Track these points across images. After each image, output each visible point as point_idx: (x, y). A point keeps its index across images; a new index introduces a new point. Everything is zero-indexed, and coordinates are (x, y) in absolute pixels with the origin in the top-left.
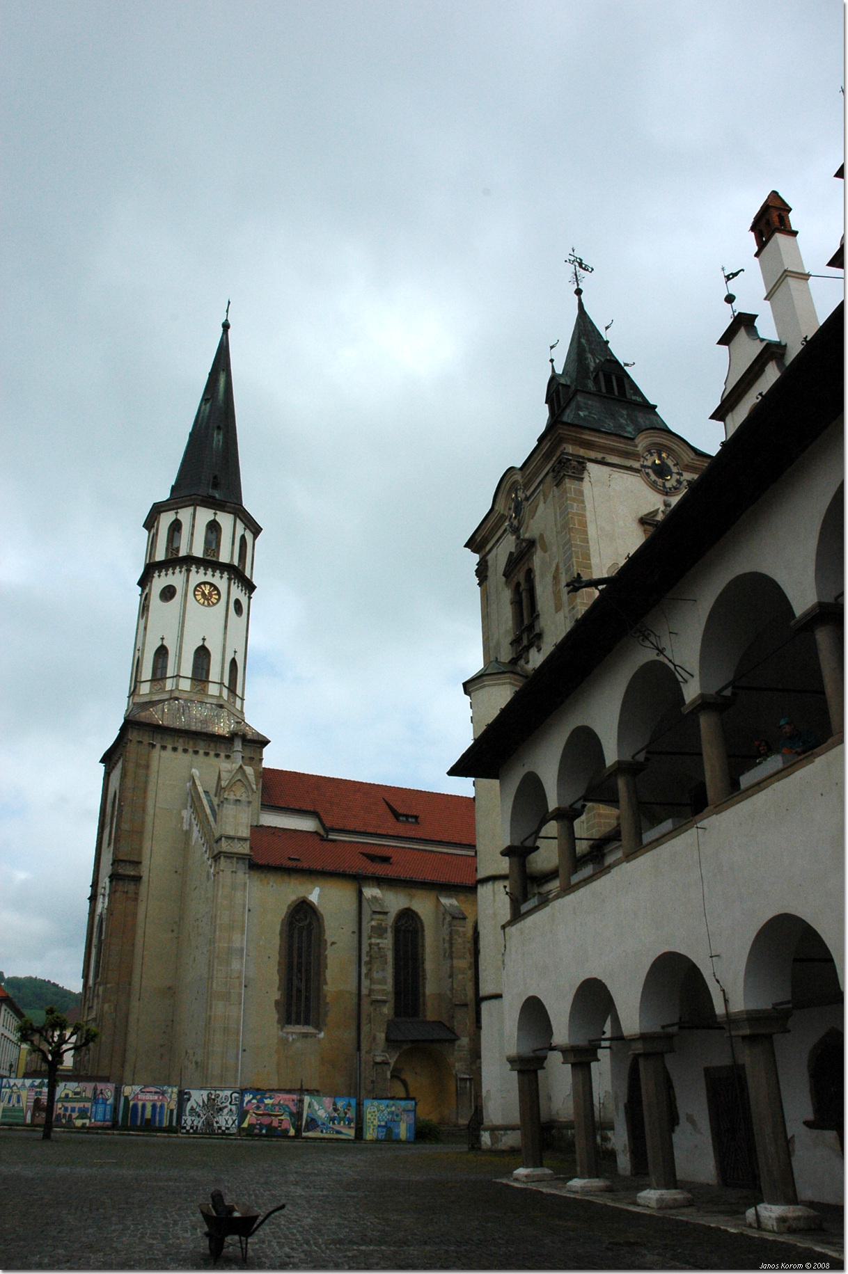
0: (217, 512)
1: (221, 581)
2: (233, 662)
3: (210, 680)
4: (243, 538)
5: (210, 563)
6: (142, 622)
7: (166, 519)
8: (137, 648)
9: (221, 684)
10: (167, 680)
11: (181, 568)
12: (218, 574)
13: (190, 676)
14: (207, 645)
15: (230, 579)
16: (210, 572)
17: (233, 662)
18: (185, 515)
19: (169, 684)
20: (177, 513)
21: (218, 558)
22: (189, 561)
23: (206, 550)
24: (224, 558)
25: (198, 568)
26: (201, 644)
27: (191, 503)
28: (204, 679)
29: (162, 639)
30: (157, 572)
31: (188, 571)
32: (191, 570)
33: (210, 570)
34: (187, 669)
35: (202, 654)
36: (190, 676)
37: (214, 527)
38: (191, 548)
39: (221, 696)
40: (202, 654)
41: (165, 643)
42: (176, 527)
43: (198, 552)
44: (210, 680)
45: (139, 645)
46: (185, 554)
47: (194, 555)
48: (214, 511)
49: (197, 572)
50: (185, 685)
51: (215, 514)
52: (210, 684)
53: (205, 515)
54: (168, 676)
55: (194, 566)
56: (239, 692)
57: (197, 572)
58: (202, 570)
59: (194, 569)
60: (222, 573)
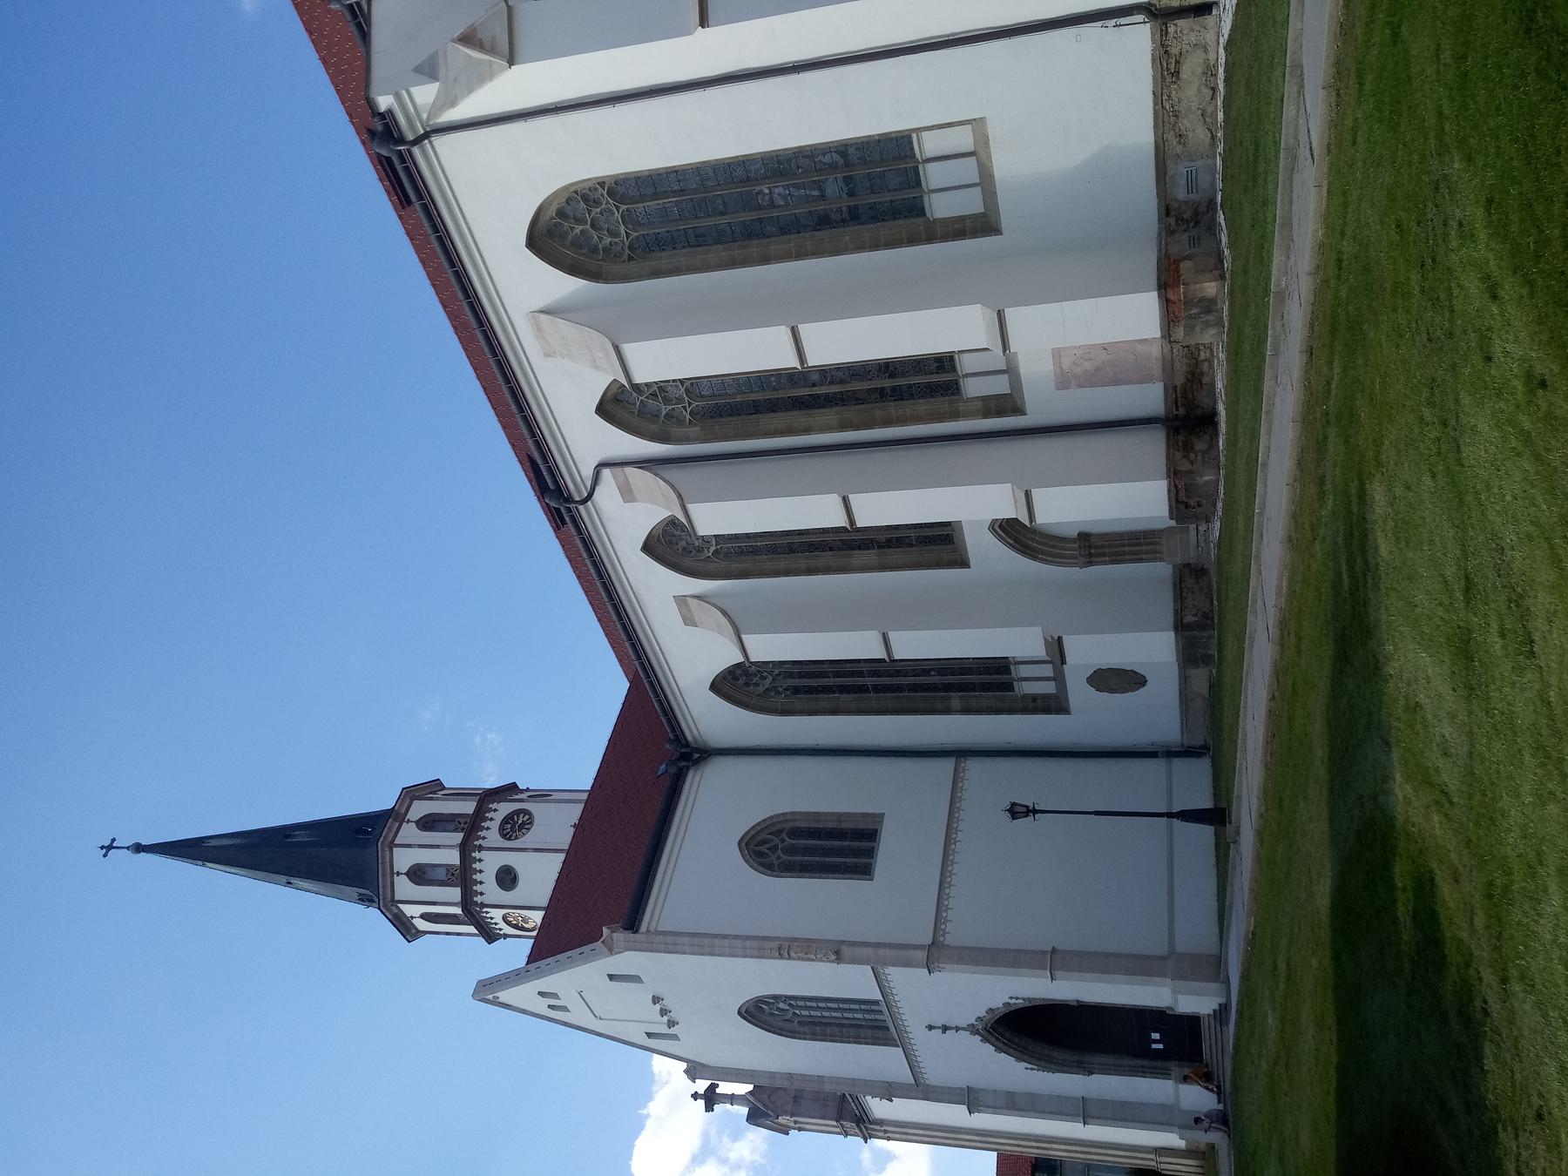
0: (395, 871)
1: (489, 864)
5: (463, 877)
12: (477, 866)
15: (480, 848)
20: (412, 918)
24: (453, 857)
31: (483, 905)
37: (419, 875)
43: (455, 893)
46: (460, 909)
47: (460, 900)
51: (398, 874)
57: (482, 894)
59: (478, 899)
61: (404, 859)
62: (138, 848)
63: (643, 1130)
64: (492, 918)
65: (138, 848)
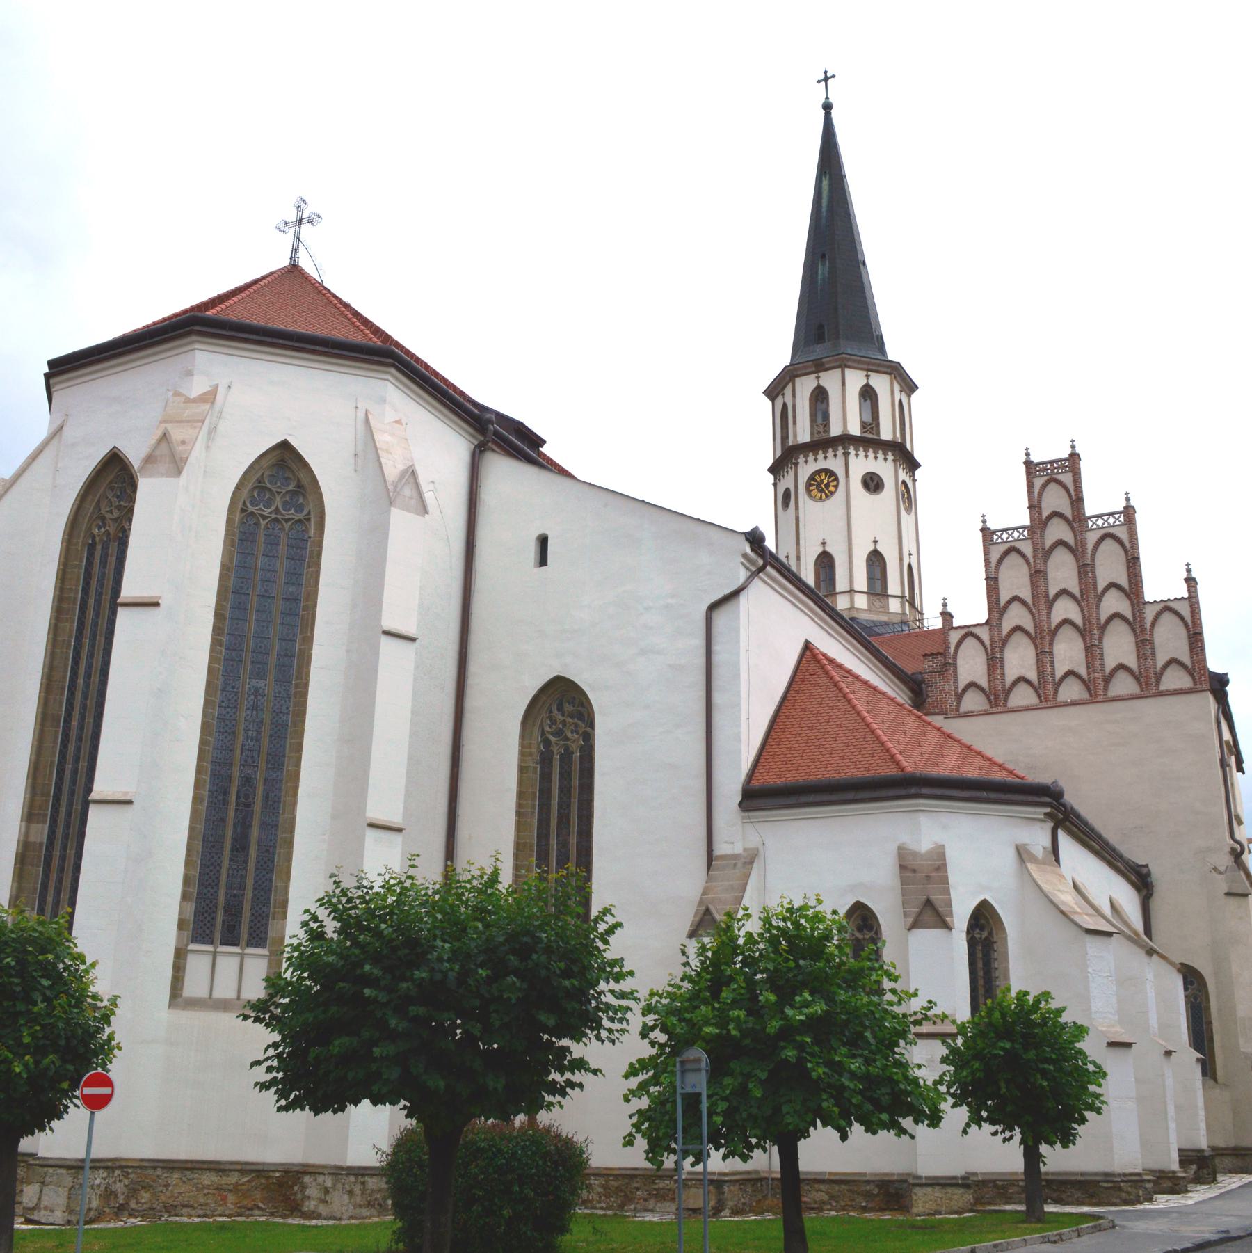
0: (869, 373)
1: (884, 467)
2: (910, 566)
3: (889, 593)
4: (900, 402)
5: (869, 441)
7: (805, 386)
9: (903, 597)
11: (835, 450)
13: (866, 590)
14: (880, 548)
16: (871, 454)
17: (910, 566)
18: (830, 380)
20: (818, 378)
21: (878, 433)
22: (846, 440)
23: (864, 425)
24: (886, 434)
25: (857, 450)
27: (838, 363)
28: (879, 591)
29: (824, 544)
30: (801, 456)
31: (846, 454)
32: (849, 453)
33: (871, 450)
34: (861, 583)
35: (876, 560)
36: (866, 590)
37: (868, 394)
39: (904, 613)
40: (876, 560)
41: (828, 549)
42: (820, 396)
43: (855, 429)
44: (889, 593)
48: (865, 373)
49: (857, 455)
50: (861, 602)
51: (868, 376)
52: (890, 599)
53: (856, 380)
54: (838, 590)
55: (852, 447)
56: (917, 604)
57: (857, 455)
58: (861, 453)
59: (852, 451)
60: (885, 454)
61: (881, 383)
63: (1227, 696)
64: (825, 458)
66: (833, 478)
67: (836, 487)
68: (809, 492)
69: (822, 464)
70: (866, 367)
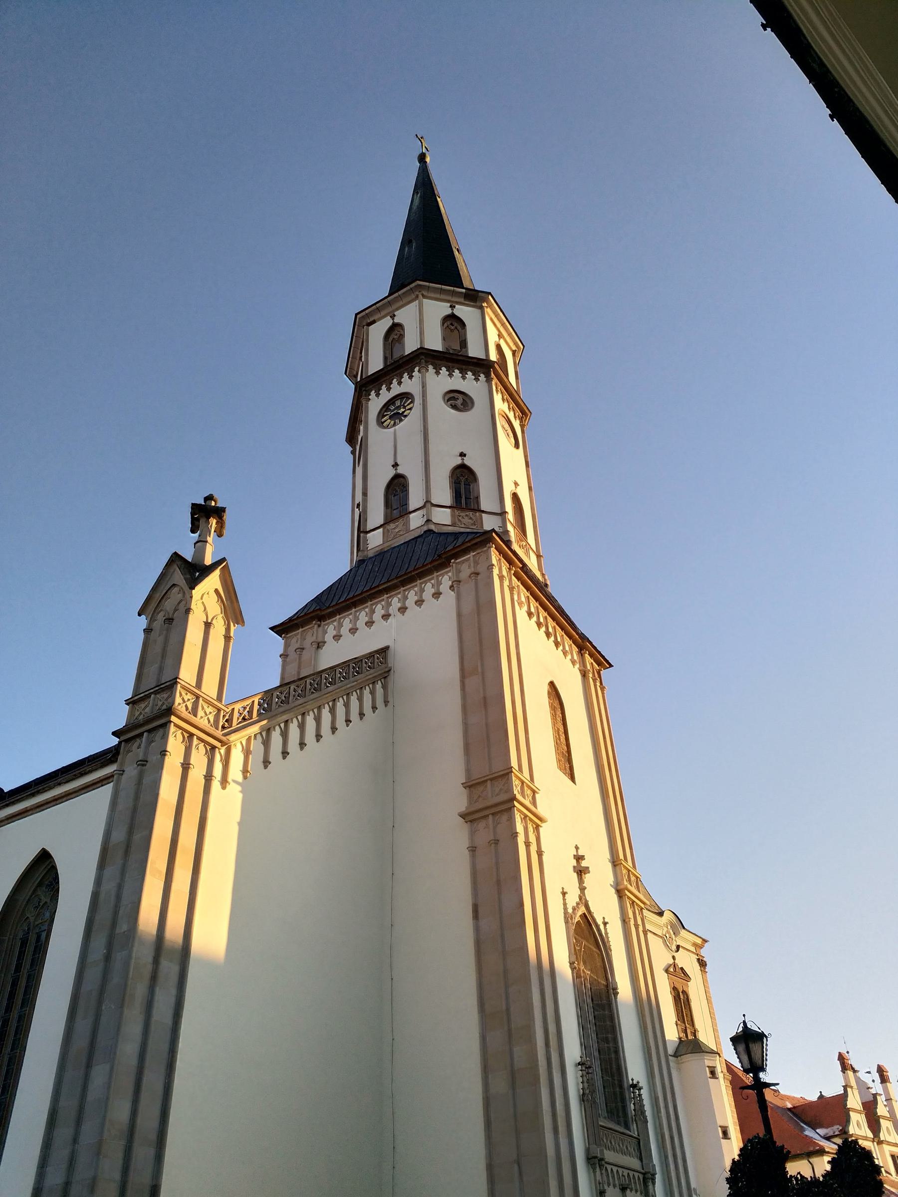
6: (359, 470)
7: (377, 332)
8: (357, 502)
10: (412, 515)
14: (467, 461)
18: (406, 315)
19: (416, 521)
20: (393, 317)
26: (459, 461)
36: (448, 503)
38: (422, 342)
41: (400, 470)
45: (359, 498)
48: (449, 305)
51: (452, 307)
54: (411, 508)
57: (438, 373)
62: (422, 158)
65: (422, 158)
66: (410, 400)
67: (410, 409)
68: (380, 423)
69: (396, 389)
70: (449, 298)
